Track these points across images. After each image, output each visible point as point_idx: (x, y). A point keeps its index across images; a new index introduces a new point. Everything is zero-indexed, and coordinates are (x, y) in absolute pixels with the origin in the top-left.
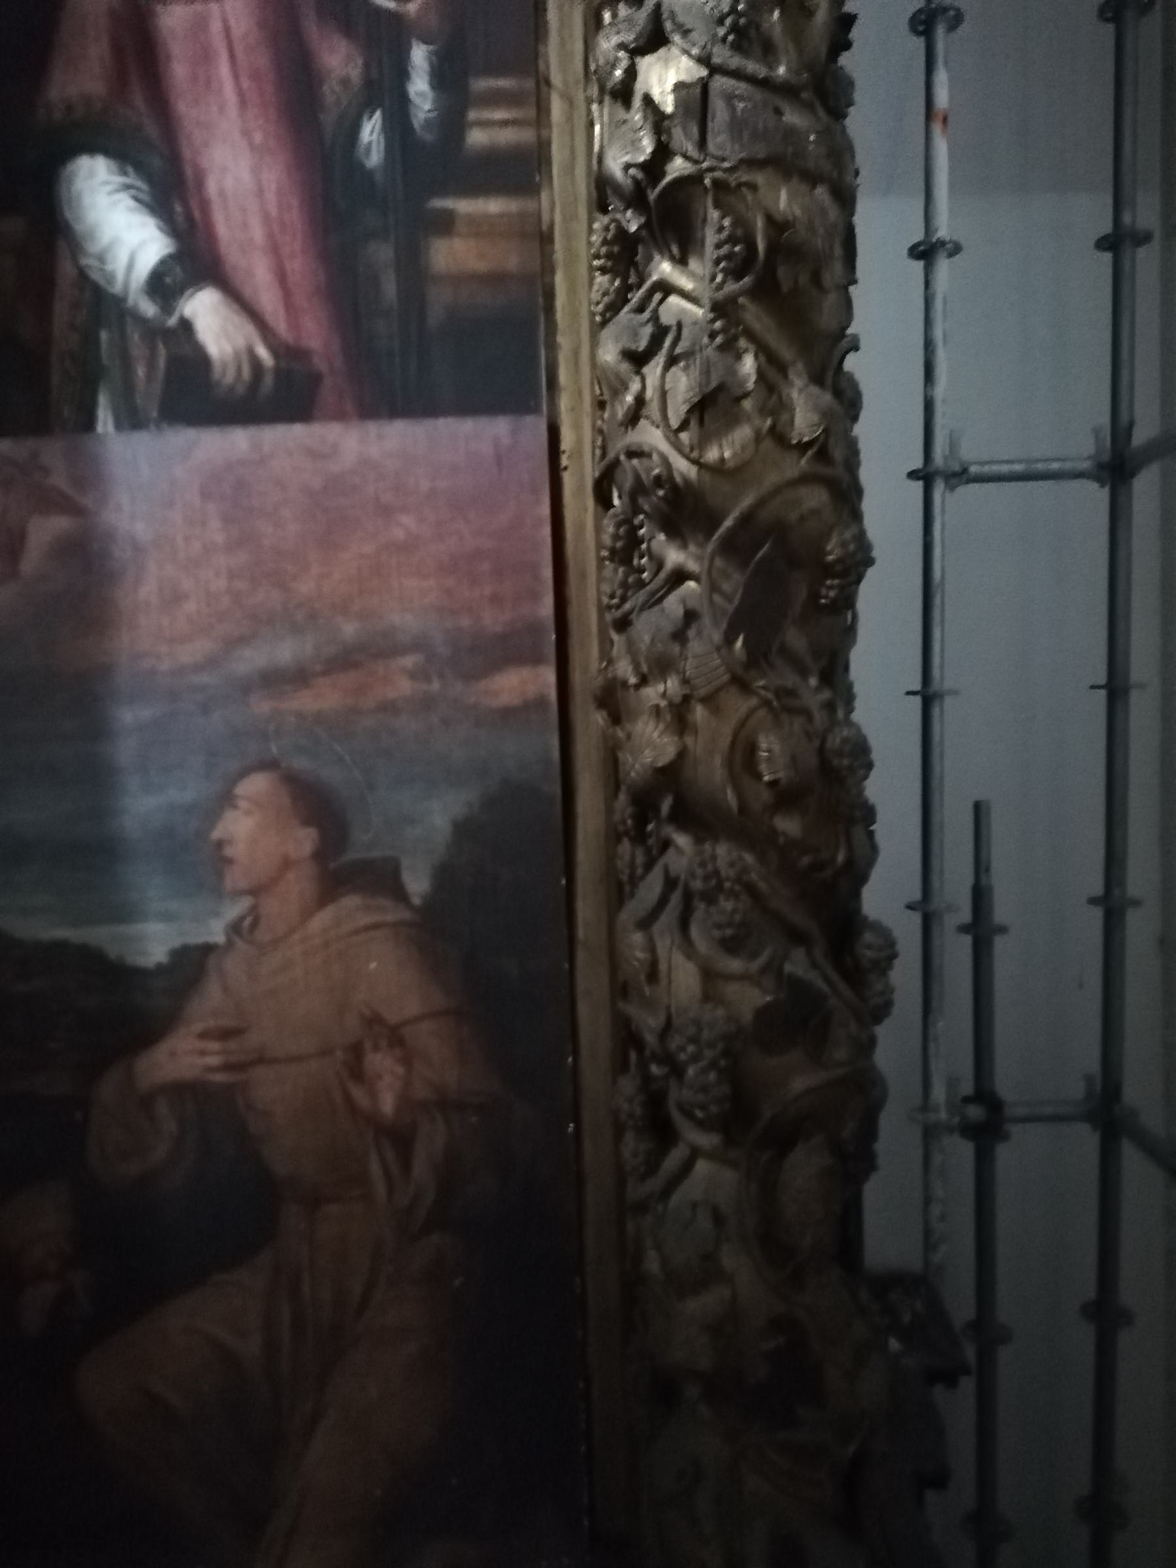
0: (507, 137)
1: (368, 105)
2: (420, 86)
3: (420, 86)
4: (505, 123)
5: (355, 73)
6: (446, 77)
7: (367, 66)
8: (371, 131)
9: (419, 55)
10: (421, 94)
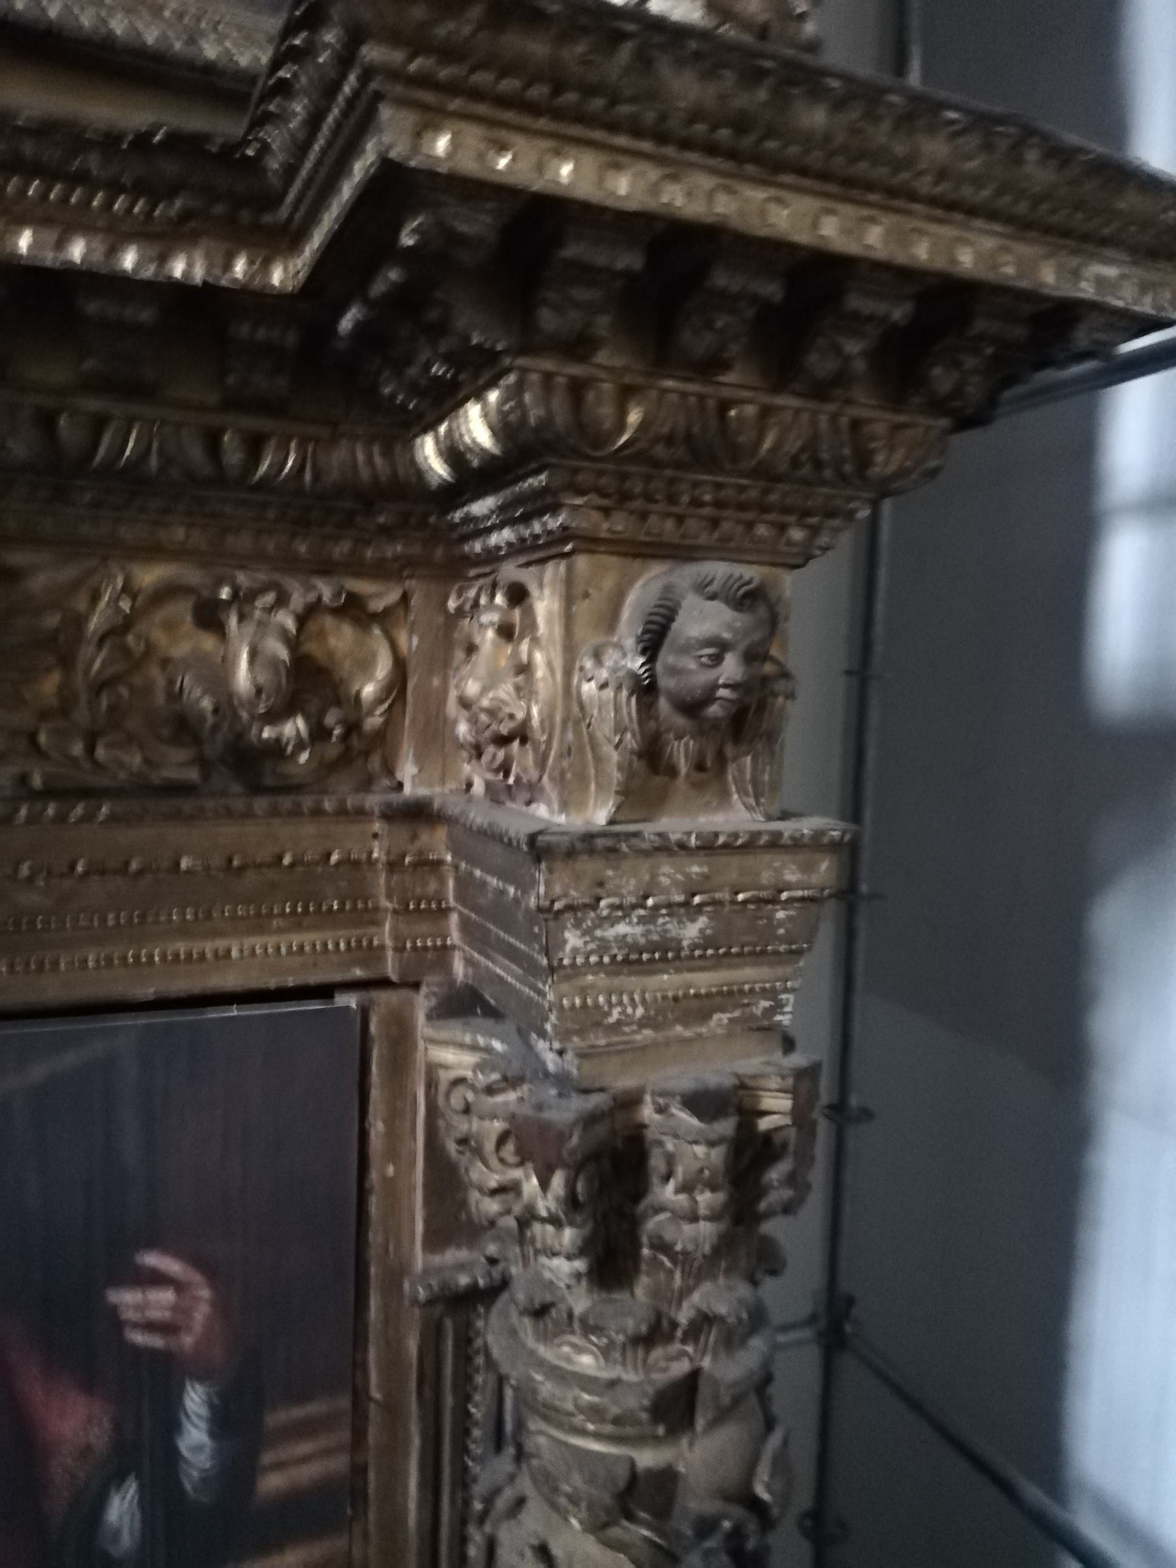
0: (307, 1473)
1: (118, 1479)
2: (195, 1438)
3: (195, 1438)
4: (305, 1459)
5: (99, 1436)
6: (234, 1422)
7: (117, 1427)
8: (121, 1509)
9: (195, 1399)
10: (199, 1448)
